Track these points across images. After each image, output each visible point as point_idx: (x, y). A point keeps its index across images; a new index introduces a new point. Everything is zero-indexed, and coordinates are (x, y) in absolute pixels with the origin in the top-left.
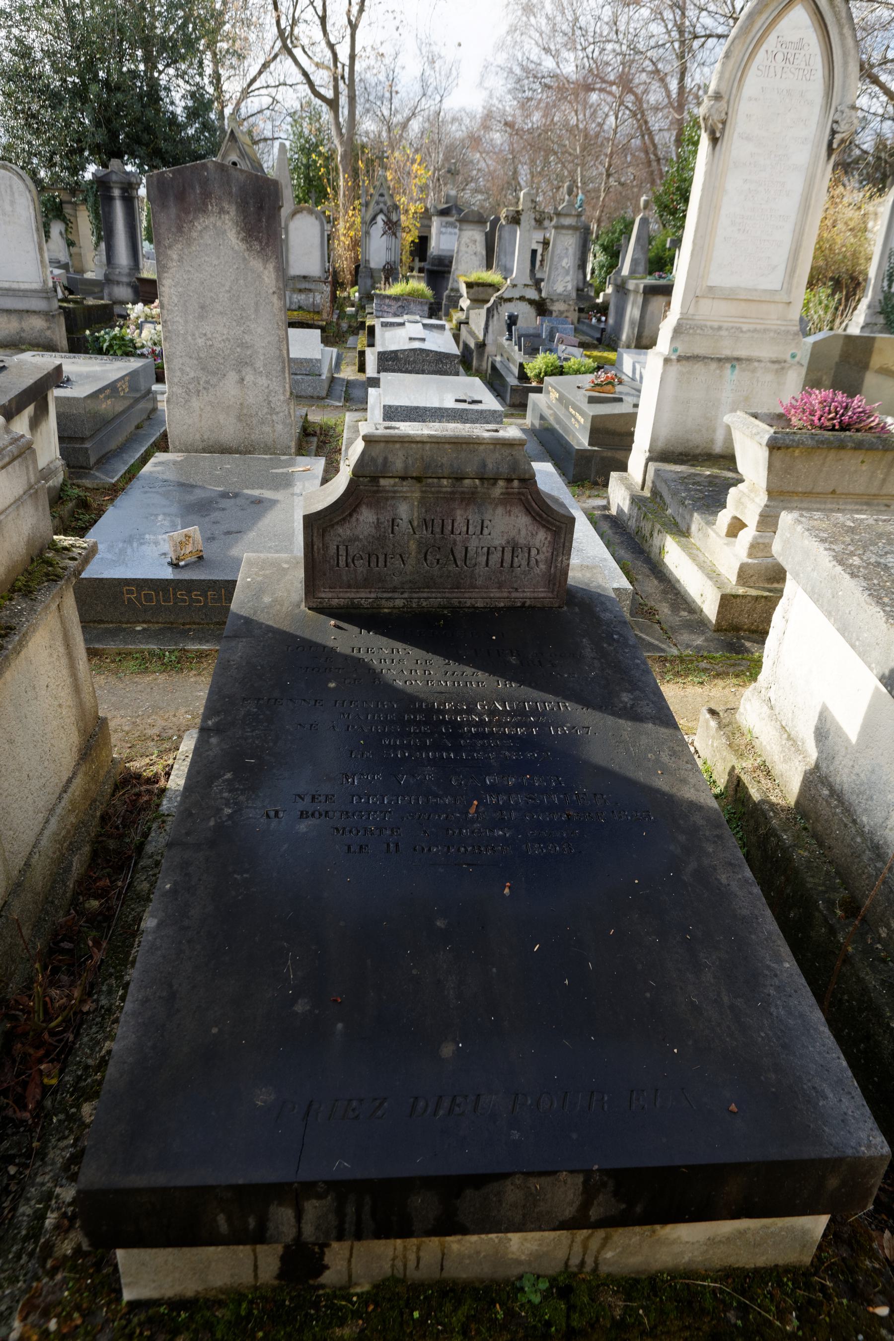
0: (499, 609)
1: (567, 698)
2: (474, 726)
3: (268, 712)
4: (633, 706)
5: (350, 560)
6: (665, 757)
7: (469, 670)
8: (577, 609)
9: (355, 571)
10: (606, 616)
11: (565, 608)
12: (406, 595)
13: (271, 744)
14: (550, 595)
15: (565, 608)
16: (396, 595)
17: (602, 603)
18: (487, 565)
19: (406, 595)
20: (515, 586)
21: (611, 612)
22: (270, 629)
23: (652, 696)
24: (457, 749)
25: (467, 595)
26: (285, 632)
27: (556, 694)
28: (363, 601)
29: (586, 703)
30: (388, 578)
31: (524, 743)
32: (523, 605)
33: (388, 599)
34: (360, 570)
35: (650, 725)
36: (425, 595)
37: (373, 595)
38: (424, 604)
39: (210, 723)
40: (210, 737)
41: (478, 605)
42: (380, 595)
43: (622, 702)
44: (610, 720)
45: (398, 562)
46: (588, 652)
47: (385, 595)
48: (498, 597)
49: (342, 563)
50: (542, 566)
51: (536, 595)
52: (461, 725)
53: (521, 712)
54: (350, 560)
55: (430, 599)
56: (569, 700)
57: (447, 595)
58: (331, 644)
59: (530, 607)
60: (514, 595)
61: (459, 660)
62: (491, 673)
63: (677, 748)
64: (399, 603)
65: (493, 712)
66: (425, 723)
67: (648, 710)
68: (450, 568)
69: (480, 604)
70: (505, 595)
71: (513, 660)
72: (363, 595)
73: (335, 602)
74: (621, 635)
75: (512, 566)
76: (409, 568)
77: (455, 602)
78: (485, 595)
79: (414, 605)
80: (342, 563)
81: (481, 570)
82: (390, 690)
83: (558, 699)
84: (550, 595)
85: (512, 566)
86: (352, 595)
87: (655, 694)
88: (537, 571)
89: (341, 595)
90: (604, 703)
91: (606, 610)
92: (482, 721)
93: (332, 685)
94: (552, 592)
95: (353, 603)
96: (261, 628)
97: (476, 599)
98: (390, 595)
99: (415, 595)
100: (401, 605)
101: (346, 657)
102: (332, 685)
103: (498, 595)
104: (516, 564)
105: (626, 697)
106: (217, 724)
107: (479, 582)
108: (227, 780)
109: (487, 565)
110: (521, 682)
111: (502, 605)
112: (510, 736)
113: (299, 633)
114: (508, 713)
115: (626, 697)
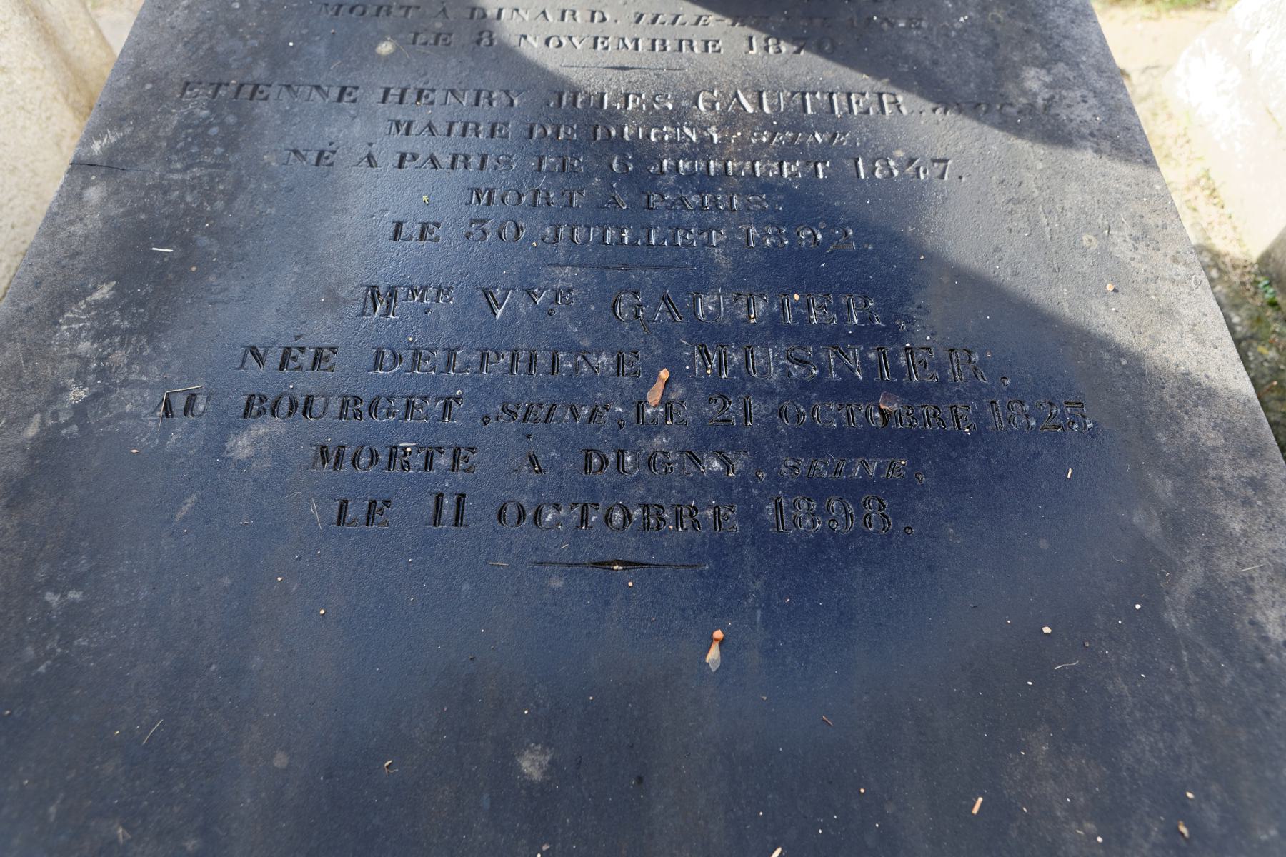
1: (900, 82)
2: (684, 156)
3: (231, 119)
6: (1122, 247)
13: (220, 204)
23: (1093, 76)
24: (641, 218)
27: (876, 73)
29: (943, 96)
31: (795, 204)
35: (1089, 155)
39: (96, 146)
40: (87, 184)
43: (1025, 93)
44: (996, 139)
52: (655, 154)
53: (794, 120)
56: (907, 88)
62: (739, 17)
63: (1151, 220)
65: (730, 120)
66: (577, 148)
67: (1084, 113)
82: (509, 58)
83: (879, 86)
87: (1100, 71)
90: (984, 100)
92: (705, 141)
93: (385, 48)
102: (385, 48)
105: (1034, 80)
106: (112, 151)
108: (98, 305)
110: (801, 42)
112: (766, 186)
114: (765, 122)
115: (1034, 80)
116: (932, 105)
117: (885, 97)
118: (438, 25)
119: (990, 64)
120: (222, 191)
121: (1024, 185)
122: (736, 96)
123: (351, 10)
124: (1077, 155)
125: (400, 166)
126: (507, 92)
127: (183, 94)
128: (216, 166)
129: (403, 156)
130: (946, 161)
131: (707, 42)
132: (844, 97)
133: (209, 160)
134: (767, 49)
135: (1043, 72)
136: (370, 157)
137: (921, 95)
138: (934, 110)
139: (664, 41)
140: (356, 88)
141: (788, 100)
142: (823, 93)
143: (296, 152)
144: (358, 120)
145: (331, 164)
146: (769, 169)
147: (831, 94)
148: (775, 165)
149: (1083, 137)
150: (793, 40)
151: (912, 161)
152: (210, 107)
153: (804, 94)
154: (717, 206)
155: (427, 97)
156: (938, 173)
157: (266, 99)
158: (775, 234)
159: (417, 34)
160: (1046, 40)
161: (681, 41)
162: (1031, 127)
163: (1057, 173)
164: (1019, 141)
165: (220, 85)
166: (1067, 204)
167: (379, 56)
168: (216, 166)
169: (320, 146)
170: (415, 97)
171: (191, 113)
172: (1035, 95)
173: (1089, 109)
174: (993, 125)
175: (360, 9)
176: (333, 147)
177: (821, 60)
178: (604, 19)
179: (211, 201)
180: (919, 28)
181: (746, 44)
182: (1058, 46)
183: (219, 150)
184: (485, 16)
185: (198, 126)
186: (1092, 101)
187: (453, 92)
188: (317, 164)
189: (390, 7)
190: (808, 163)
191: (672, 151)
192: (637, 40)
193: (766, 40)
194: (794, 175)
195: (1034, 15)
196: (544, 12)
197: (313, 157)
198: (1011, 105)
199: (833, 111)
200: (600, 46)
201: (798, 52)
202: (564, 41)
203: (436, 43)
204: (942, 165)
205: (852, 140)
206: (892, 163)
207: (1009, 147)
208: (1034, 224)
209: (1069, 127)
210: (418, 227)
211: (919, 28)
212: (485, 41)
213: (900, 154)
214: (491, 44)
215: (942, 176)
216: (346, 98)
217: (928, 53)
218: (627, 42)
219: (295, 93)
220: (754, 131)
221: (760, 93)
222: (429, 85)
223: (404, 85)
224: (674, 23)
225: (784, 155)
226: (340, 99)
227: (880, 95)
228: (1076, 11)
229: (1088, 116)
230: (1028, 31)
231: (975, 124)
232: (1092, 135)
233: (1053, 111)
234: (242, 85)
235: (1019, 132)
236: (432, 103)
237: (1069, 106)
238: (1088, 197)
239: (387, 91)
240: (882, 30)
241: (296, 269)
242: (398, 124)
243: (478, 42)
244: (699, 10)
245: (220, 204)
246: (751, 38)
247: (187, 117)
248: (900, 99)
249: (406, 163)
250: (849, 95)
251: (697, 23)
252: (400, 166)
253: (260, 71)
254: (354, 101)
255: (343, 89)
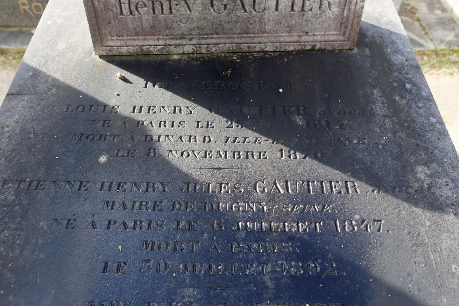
0: (288, 53)
1: (356, 175)
4: (430, 186)
5: (133, 8)
7: (252, 135)
8: (367, 52)
9: (141, 18)
10: (397, 59)
11: (356, 50)
12: (194, 42)
13: (17, 252)
14: (341, 38)
15: (356, 50)
16: (184, 42)
17: (393, 43)
18: (277, 9)
19: (194, 42)
20: (306, 29)
21: (402, 54)
22: (57, 84)
23: (451, 170)
25: (256, 40)
26: (69, 87)
28: (152, 48)
29: (377, 183)
30: (175, 25)
31: (305, 248)
32: (313, 49)
33: (176, 46)
34: (145, 17)
35: (452, 217)
36: (214, 41)
37: (161, 42)
38: (214, 50)
41: (268, 49)
42: (168, 42)
43: (418, 180)
45: (183, 9)
46: (380, 108)
47: (174, 42)
48: (289, 41)
49: (126, 11)
50: (335, 9)
51: (326, 38)
53: (304, 198)
54: (133, 8)
55: (220, 45)
56: (359, 179)
57: (236, 40)
58: (112, 102)
59: (320, 50)
60: (304, 38)
61: (241, 120)
62: (276, 139)
64: (188, 49)
65: (272, 198)
68: (239, 14)
69: (269, 48)
70: (295, 39)
71: (299, 120)
72: (151, 42)
73: (124, 50)
74: (414, 84)
75: (303, 10)
76: (195, 14)
77: (245, 47)
78: (274, 40)
79: (204, 51)
80: (126, 11)
81: (270, 14)
82: (163, 164)
83: (346, 177)
84: (341, 38)
85: (303, 10)
86: (141, 43)
88: (329, 14)
89: (129, 43)
91: (396, 51)
93: (103, 159)
94: (344, 35)
95: (142, 50)
96: (47, 82)
97: (265, 44)
98: (178, 42)
99: (204, 41)
100: (191, 51)
101: (125, 120)
103: (287, 39)
104: (306, 8)
107: (268, 27)
109: (277, 9)
110: (307, 153)
111: (292, 48)
112: (291, 238)
113: (83, 89)
115: (422, 172)
116: (372, 188)
117: (348, 183)
118: (129, 145)
119: (399, 164)
120: (18, 244)
121: (421, 235)
122: (275, 184)
123: (87, 138)
124: (446, 217)
125: (108, 228)
126: (162, 184)
127: (3, 187)
128: (16, 229)
129: (110, 222)
130: (381, 221)
131: (260, 153)
132: (328, 184)
133: (13, 226)
134: (289, 156)
135: (426, 168)
136: (93, 223)
137: (367, 182)
138: (373, 191)
139: (239, 153)
140: (88, 182)
141: (301, 186)
142: (318, 181)
143: (56, 220)
144: (88, 201)
145: (73, 228)
146: (292, 227)
147: (322, 182)
148: (295, 225)
149: (448, 206)
150: (302, 152)
151: (363, 221)
152: (16, 195)
153: (308, 182)
154: (266, 250)
155: (122, 187)
156: (377, 228)
157: (43, 189)
158: (296, 266)
159: (119, 150)
160: (426, 150)
161: (247, 152)
162: (422, 200)
163: (437, 228)
164: (416, 209)
165: (21, 181)
166: (443, 247)
167: (100, 163)
168: (16, 229)
169: (69, 217)
170: (116, 187)
171: (6, 198)
172: (423, 181)
173: (450, 189)
174: (403, 200)
175: (91, 137)
176: (75, 217)
177: (316, 163)
178: (210, 141)
179: (13, 250)
180: (364, 143)
181: (279, 154)
182: (432, 153)
183: (18, 220)
184: (152, 139)
185: (9, 206)
186: (451, 185)
187: (135, 184)
188: (67, 228)
189: (106, 135)
190: (311, 223)
191: (244, 217)
192: (226, 152)
193: (289, 152)
194: (304, 230)
195: (419, 136)
196: (181, 137)
197: (65, 223)
198: (411, 187)
199: (323, 192)
200: (208, 156)
201: (305, 158)
202: (191, 153)
203: (128, 156)
204: (379, 223)
205: (333, 209)
206: (354, 223)
207: (412, 212)
208: (427, 257)
209: (443, 199)
210: (115, 265)
211: (364, 143)
212: (152, 154)
213: (357, 217)
214: (155, 156)
215: (379, 230)
216: (83, 188)
217: (369, 158)
218: (221, 153)
219: (58, 185)
220: (284, 204)
221: (287, 182)
222: (124, 180)
223: (111, 181)
224: (244, 142)
225: (300, 218)
226: (79, 189)
227: (346, 182)
228: (440, 133)
229: (450, 194)
230: (417, 145)
231: (394, 199)
232: (452, 205)
233: (432, 191)
234: (32, 181)
235: (416, 203)
236: (125, 190)
237: (440, 188)
238: (453, 242)
239: (103, 183)
240: (346, 145)
241: (53, 292)
242: (107, 203)
243: (148, 155)
244: (256, 135)
245: (17, 252)
246: (282, 150)
247: (4, 201)
248: (356, 184)
249: (111, 226)
250: (331, 182)
251: (255, 142)
252: (108, 228)
253: (41, 174)
254: (86, 190)
255: (82, 183)
